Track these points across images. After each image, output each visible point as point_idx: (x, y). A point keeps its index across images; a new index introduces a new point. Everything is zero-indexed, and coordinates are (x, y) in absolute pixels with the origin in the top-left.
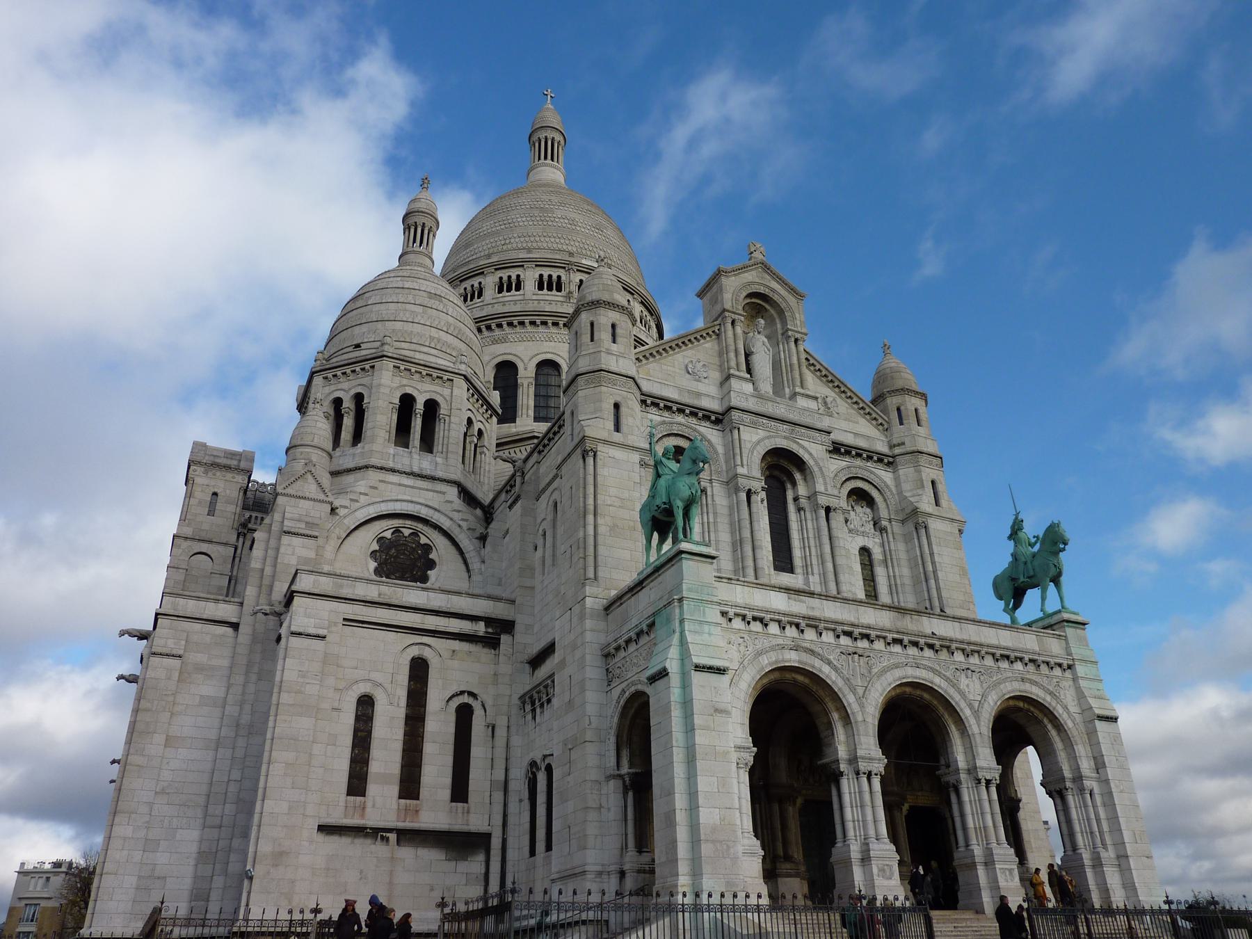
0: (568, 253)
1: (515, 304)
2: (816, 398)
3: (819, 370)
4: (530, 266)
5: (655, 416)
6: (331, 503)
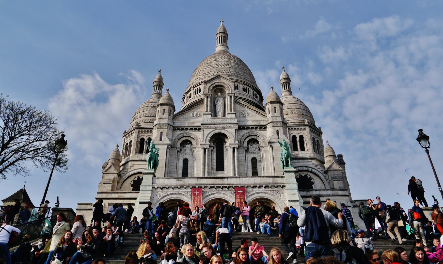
1: (197, 97)
2: (235, 114)
5: (178, 133)
6: (117, 174)
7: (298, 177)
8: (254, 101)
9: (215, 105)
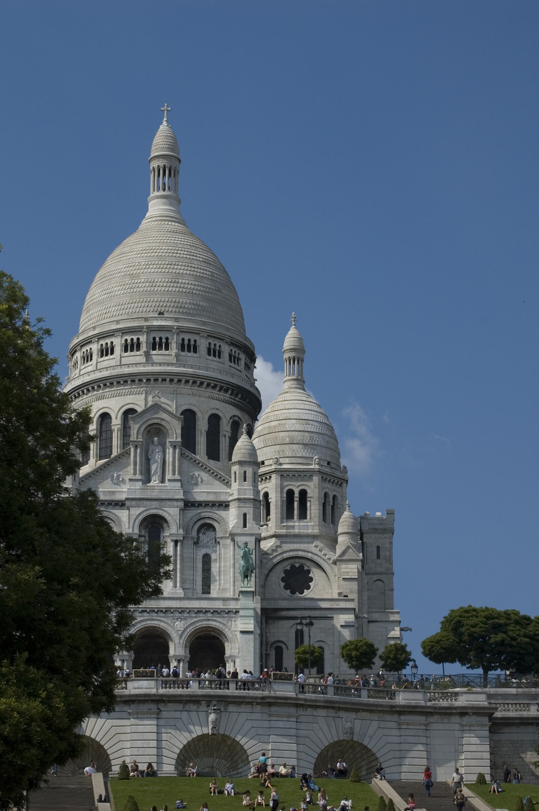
1: (107, 370)
3: (191, 458)
4: (118, 334)
7: (288, 568)
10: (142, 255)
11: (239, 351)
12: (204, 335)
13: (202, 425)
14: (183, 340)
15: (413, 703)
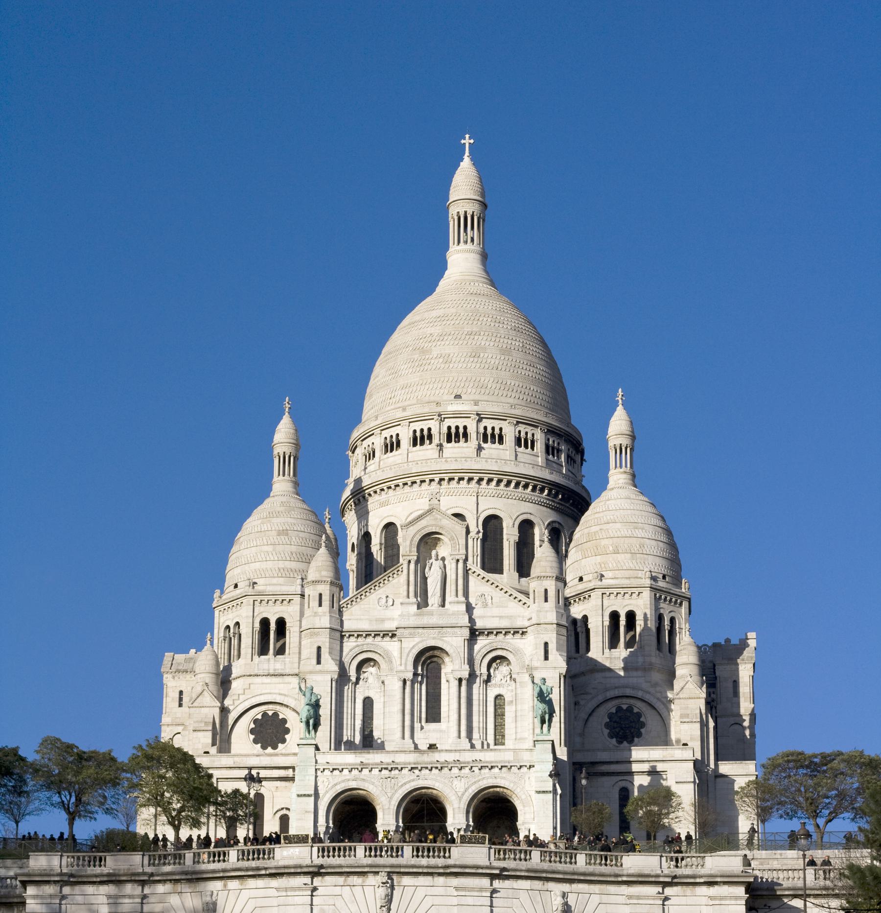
0: (435, 404)
7: (614, 710)
8: (546, 475)
9: (426, 579)
10: (435, 324)
11: (559, 440)
12: (512, 421)
13: (510, 535)
14: (485, 428)
15: (646, 872)
